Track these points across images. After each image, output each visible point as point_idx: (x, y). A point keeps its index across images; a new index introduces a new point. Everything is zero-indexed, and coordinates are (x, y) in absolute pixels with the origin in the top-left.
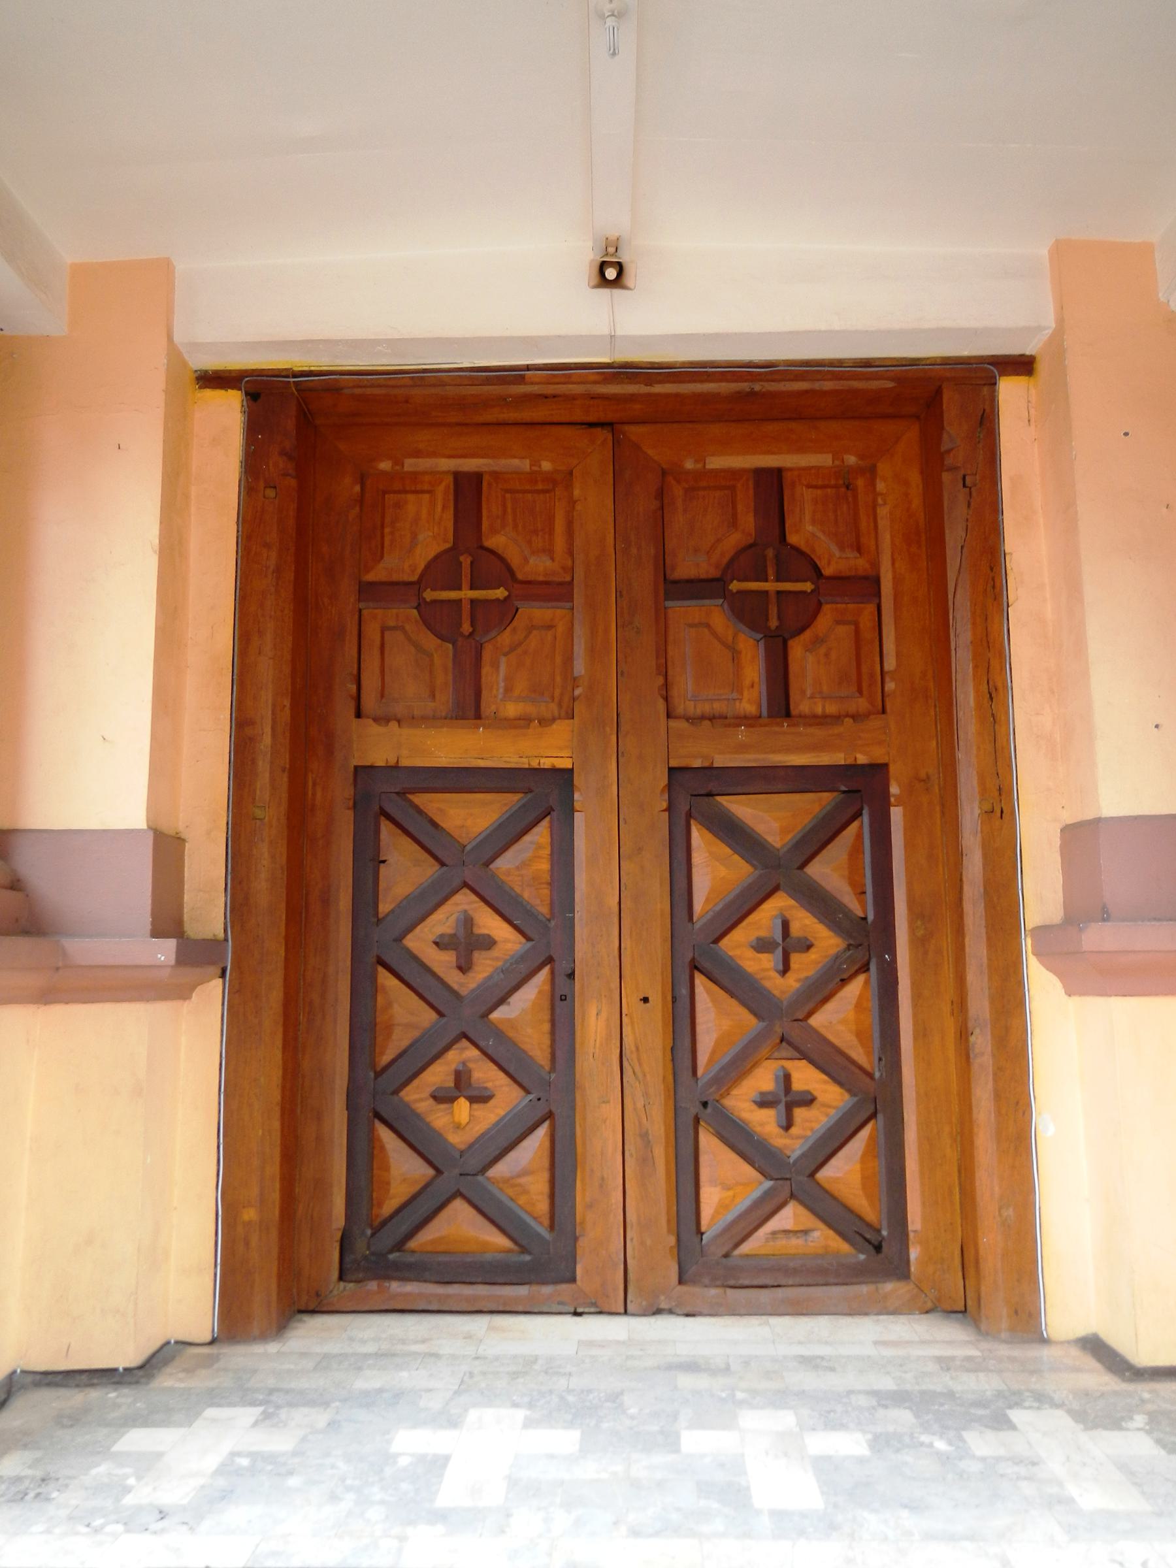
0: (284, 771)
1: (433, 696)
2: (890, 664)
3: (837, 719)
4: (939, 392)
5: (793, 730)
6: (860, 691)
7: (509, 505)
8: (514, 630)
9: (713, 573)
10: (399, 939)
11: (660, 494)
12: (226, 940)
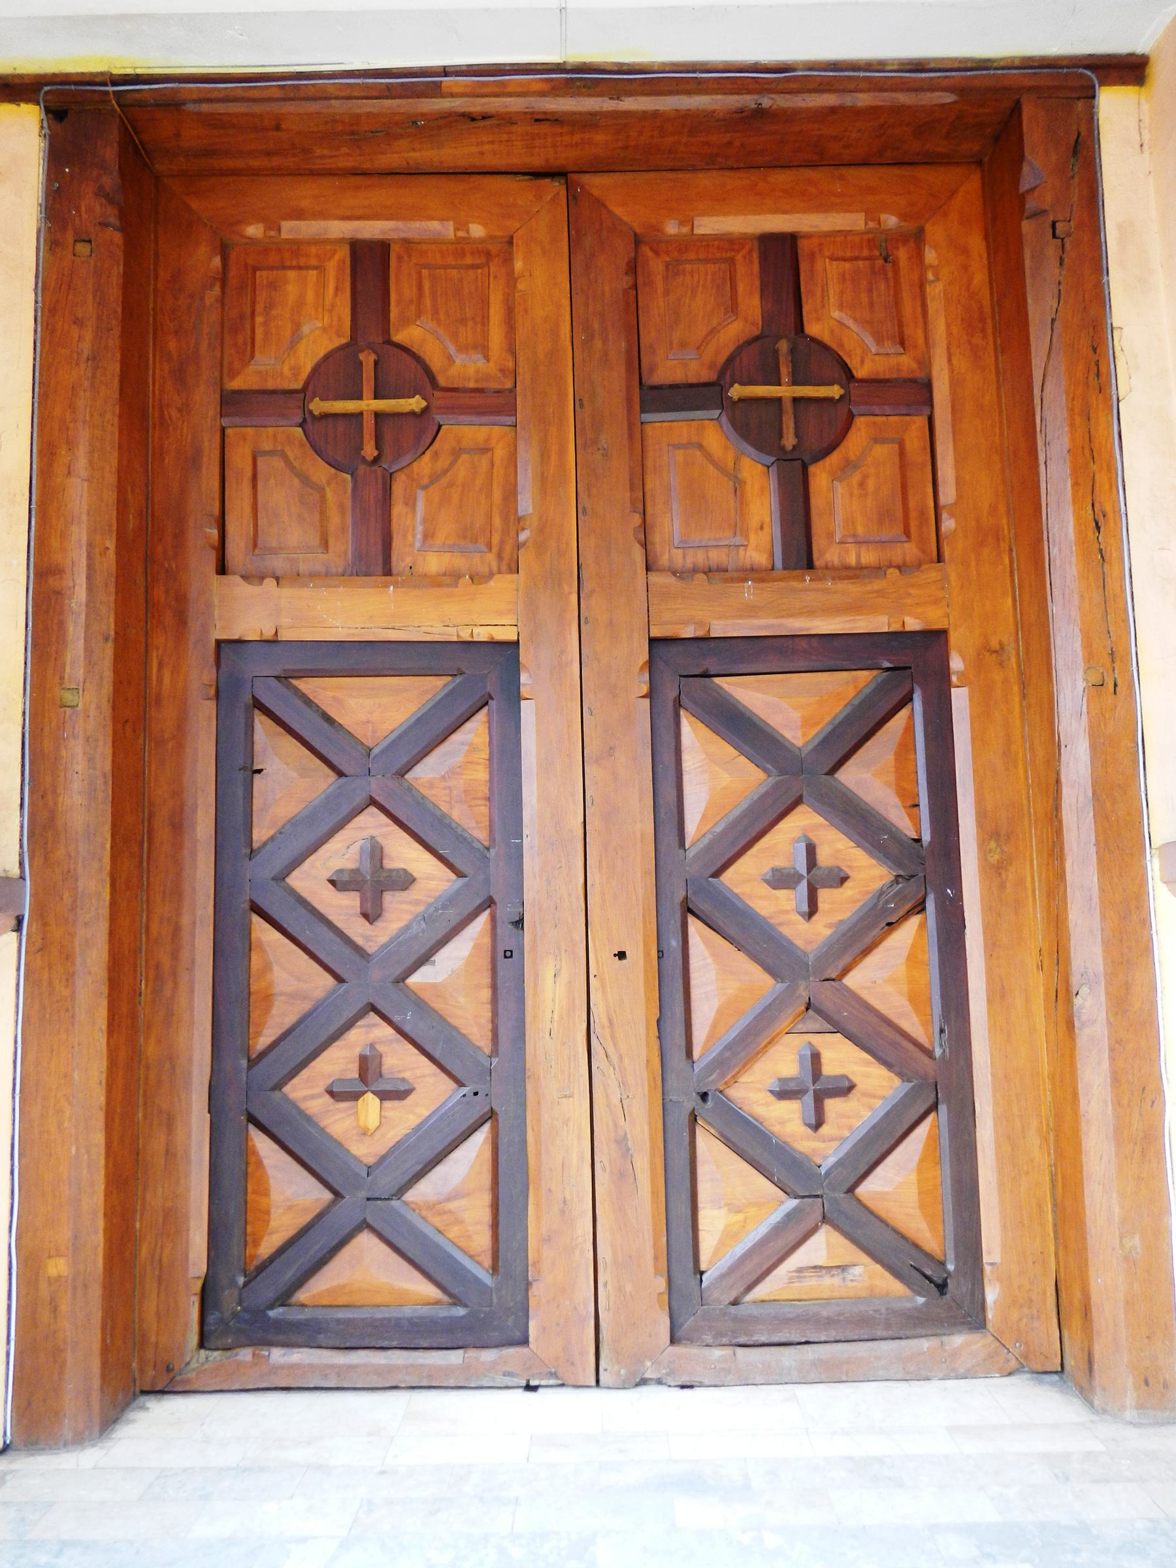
0: (106, 639)
1: (325, 544)
2: (948, 494)
3: (877, 570)
4: (1017, 109)
5: (815, 585)
6: (907, 533)
7: (427, 285)
8: (436, 455)
9: (707, 376)
10: (281, 877)
11: (633, 268)
12: (22, 878)
